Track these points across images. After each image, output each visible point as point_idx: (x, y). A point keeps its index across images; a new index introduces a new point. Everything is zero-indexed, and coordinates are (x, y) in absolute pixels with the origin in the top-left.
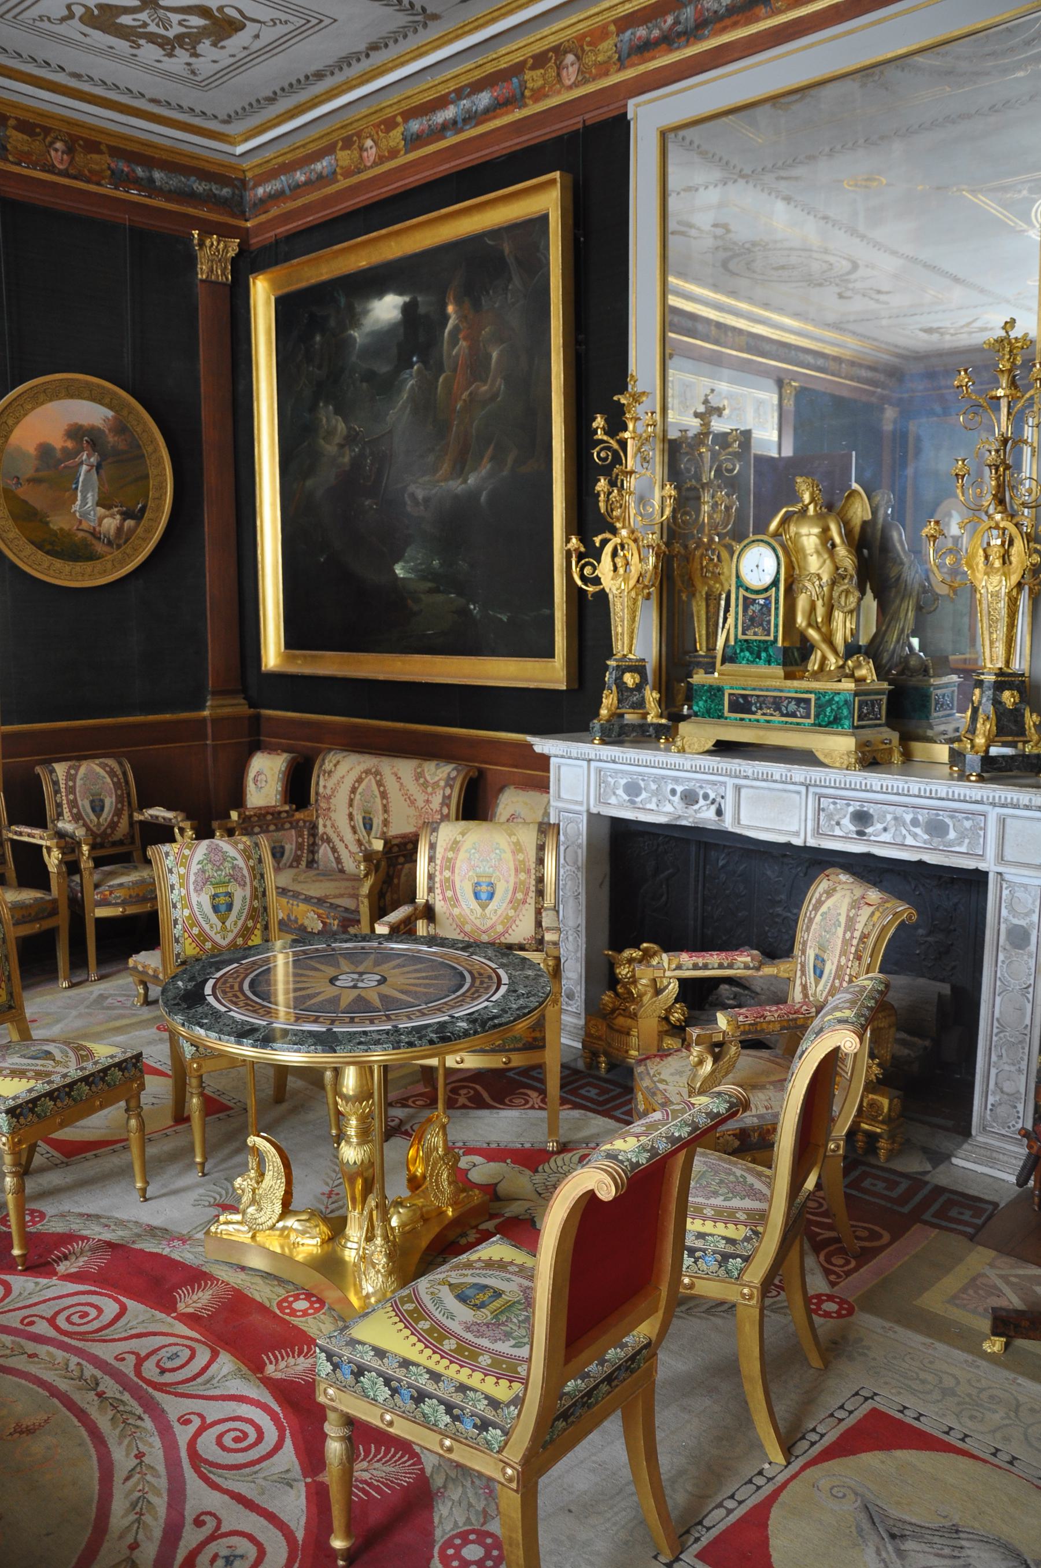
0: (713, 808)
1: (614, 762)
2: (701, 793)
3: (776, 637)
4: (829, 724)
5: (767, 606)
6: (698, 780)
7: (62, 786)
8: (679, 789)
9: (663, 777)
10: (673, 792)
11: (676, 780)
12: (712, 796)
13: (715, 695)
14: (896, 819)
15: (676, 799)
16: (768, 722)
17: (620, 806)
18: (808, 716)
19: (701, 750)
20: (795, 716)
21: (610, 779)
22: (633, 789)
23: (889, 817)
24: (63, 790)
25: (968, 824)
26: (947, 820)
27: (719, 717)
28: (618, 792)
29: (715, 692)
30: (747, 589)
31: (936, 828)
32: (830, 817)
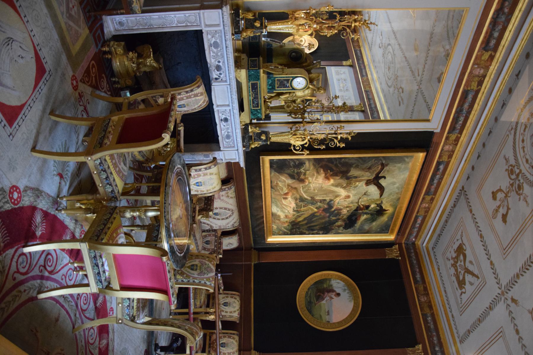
0: (217, 77)
1: (226, 47)
2: (221, 72)
3: (277, 90)
4: (252, 112)
5: (286, 87)
6: (225, 70)
7: (191, 94)
8: (221, 64)
9: (223, 57)
10: (219, 62)
11: (224, 62)
12: (221, 76)
13: (256, 78)
14: (228, 128)
15: (217, 63)
16: (250, 95)
17: (209, 40)
18: (253, 107)
19: (237, 77)
20: (253, 103)
21: (218, 35)
22: (216, 45)
23: (228, 127)
24: (188, 94)
25: (231, 143)
26: (231, 139)
27: (249, 79)
28: (213, 38)
29: (258, 78)
30: (292, 80)
31: (228, 137)
32: (223, 112)
